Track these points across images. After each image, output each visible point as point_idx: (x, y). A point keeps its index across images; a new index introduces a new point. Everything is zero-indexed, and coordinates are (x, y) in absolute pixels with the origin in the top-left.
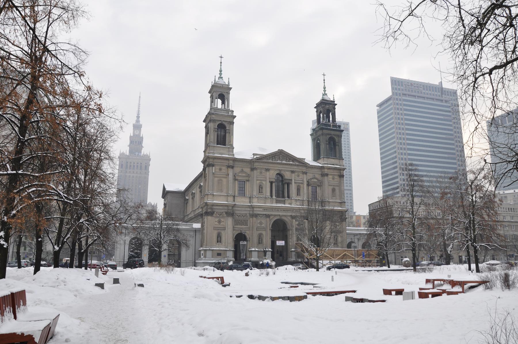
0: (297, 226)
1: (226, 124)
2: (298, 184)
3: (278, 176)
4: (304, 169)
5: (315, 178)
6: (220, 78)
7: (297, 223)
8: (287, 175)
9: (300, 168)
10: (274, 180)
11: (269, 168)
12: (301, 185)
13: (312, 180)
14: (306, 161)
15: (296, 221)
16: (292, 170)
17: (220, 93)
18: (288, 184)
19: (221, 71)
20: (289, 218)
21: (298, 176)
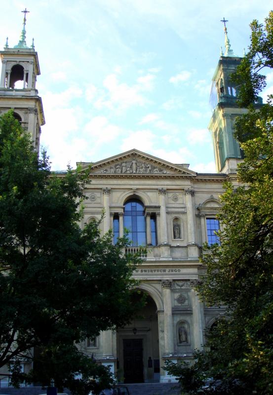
0: (176, 303)
1: (21, 113)
2: (174, 216)
3: (134, 204)
4: (187, 185)
5: (212, 200)
6: (23, 42)
7: (177, 295)
8: (150, 199)
9: (178, 182)
10: (121, 211)
11: (109, 187)
12: (181, 216)
13: (208, 205)
14: (190, 168)
15: (173, 291)
16: (160, 187)
17: (14, 64)
18: (154, 217)
19: (24, 33)
20: (159, 286)
21: (176, 199)
